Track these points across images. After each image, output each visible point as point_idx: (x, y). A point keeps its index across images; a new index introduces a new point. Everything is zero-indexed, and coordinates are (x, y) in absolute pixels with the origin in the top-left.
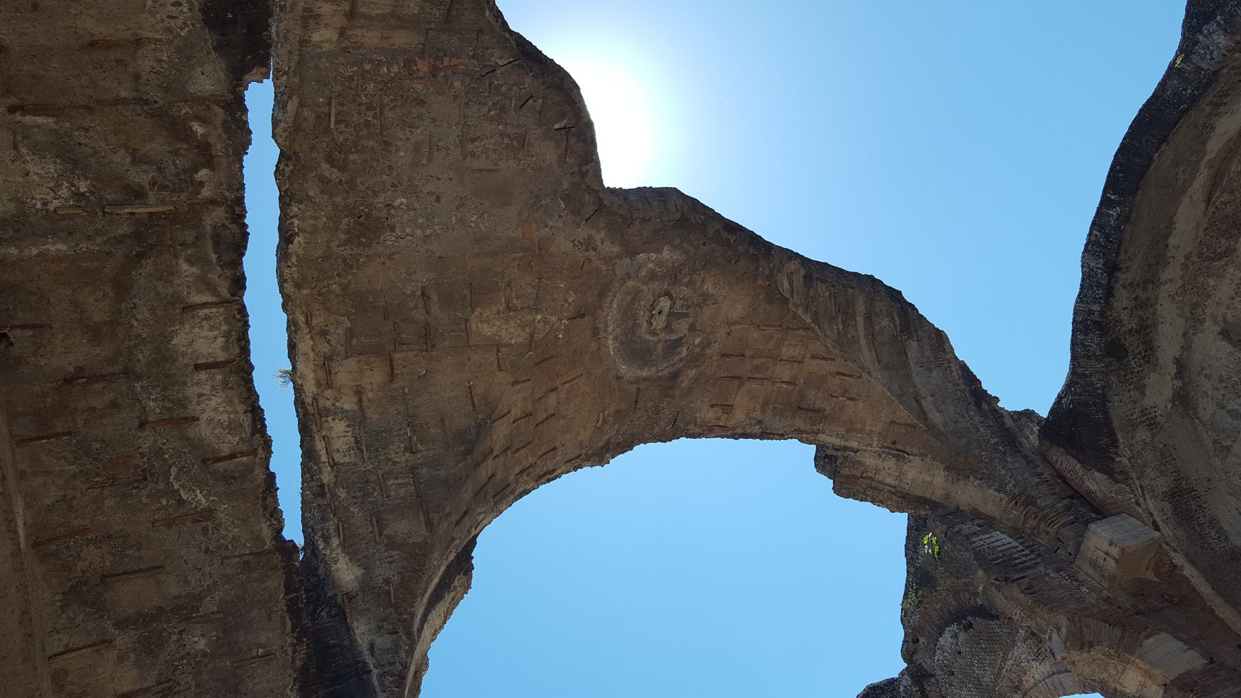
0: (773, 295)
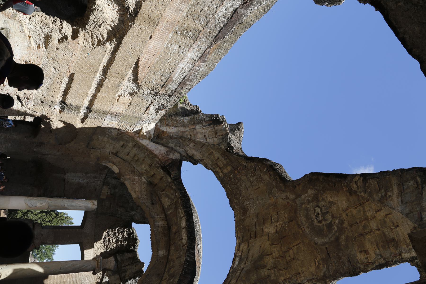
0: (351, 192)
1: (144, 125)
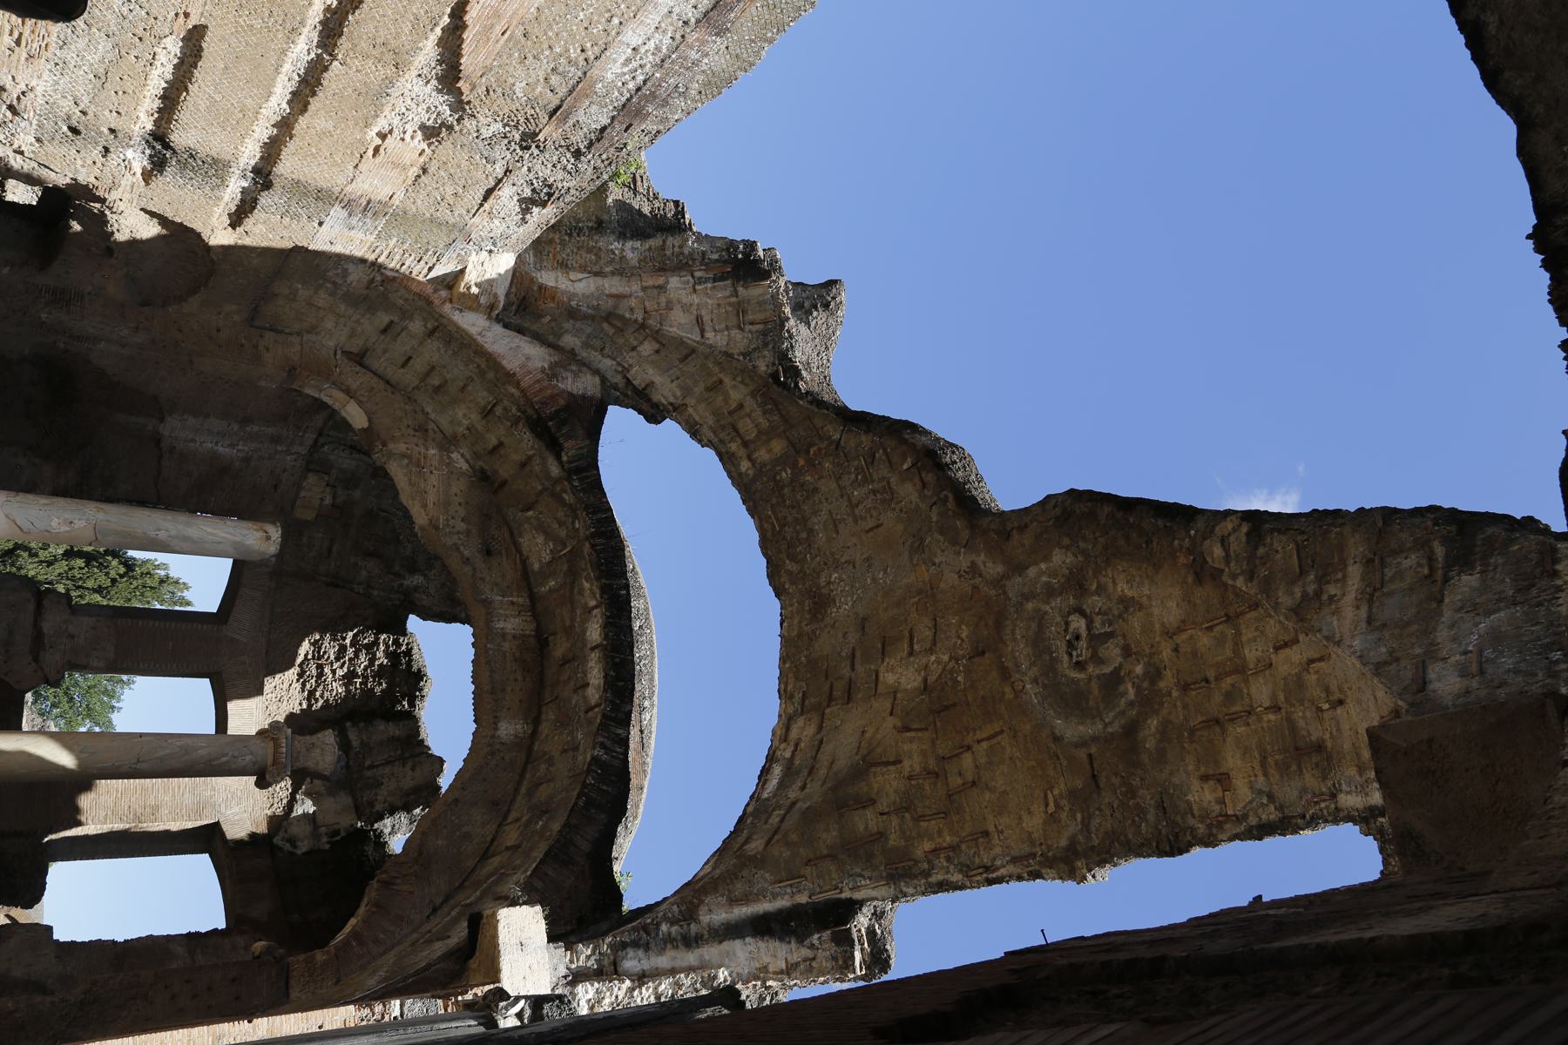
0: (1201, 572)
1: (473, 258)
